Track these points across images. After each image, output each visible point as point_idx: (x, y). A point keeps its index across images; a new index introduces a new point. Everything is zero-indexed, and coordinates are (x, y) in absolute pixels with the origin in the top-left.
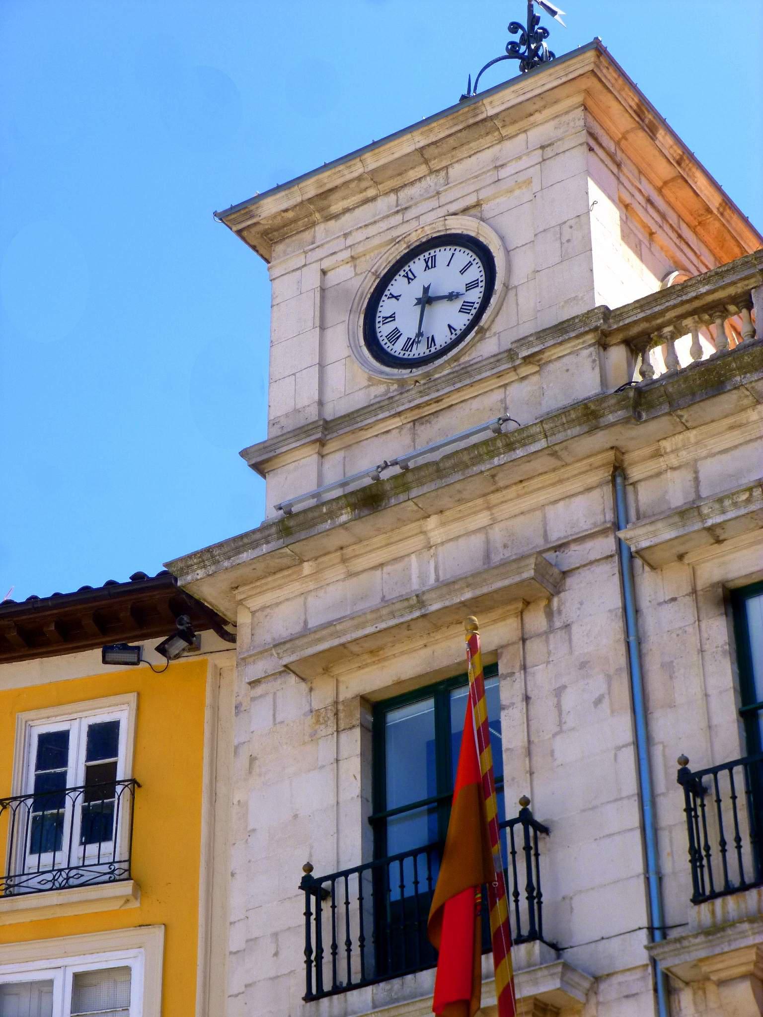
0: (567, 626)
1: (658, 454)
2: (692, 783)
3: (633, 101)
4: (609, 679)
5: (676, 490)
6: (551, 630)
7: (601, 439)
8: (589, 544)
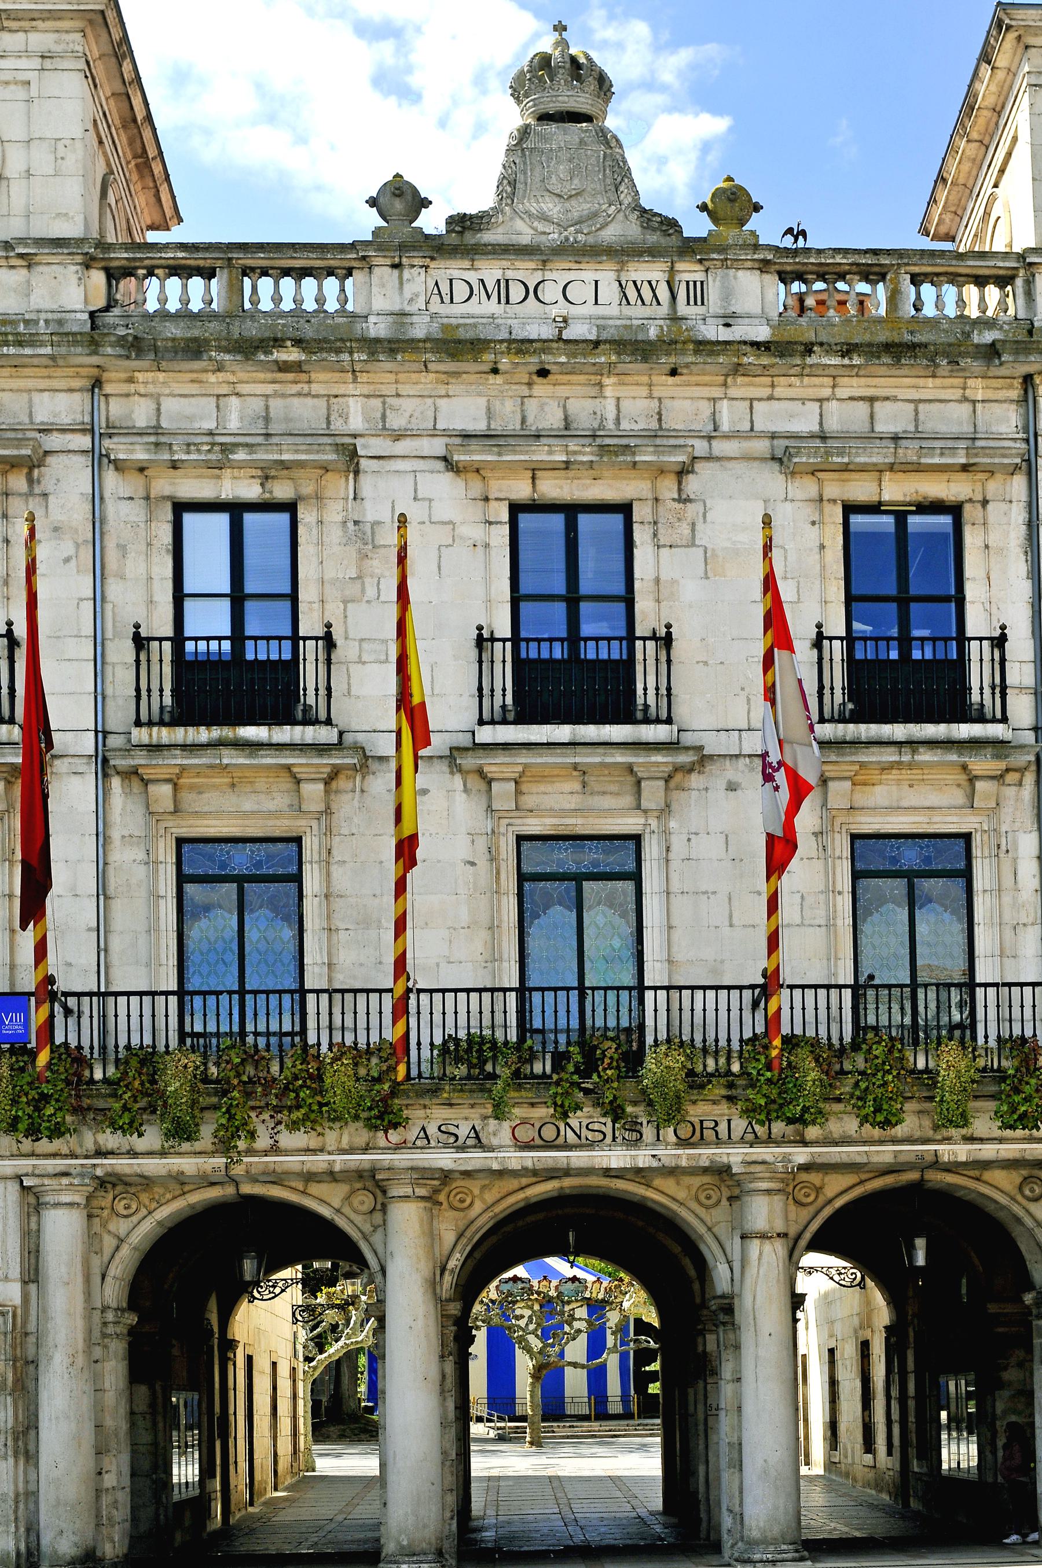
0: (45, 495)
1: (131, 380)
2: (140, 642)
3: (116, 35)
4: (77, 546)
5: (141, 414)
6: (30, 494)
7: (95, 360)
8: (69, 436)
